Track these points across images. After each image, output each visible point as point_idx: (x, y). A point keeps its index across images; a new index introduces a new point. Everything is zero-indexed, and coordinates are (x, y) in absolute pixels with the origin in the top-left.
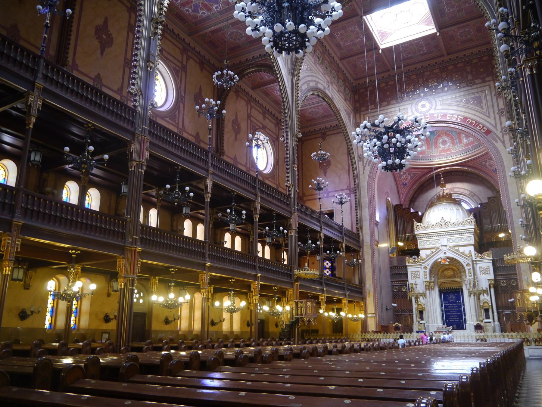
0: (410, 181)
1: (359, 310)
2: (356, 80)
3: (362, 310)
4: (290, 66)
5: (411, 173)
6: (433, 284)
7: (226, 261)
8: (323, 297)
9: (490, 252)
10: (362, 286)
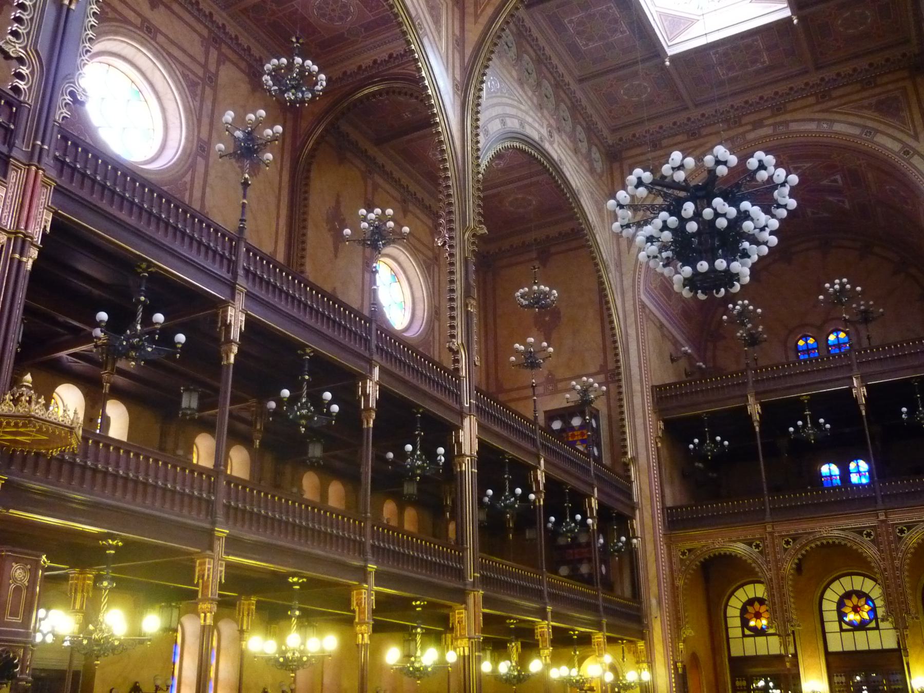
1: (634, 660)
2: (614, 130)
3: (643, 662)
4: (458, 77)
7: (273, 524)
8: (544, 627)
10: (640, 603)
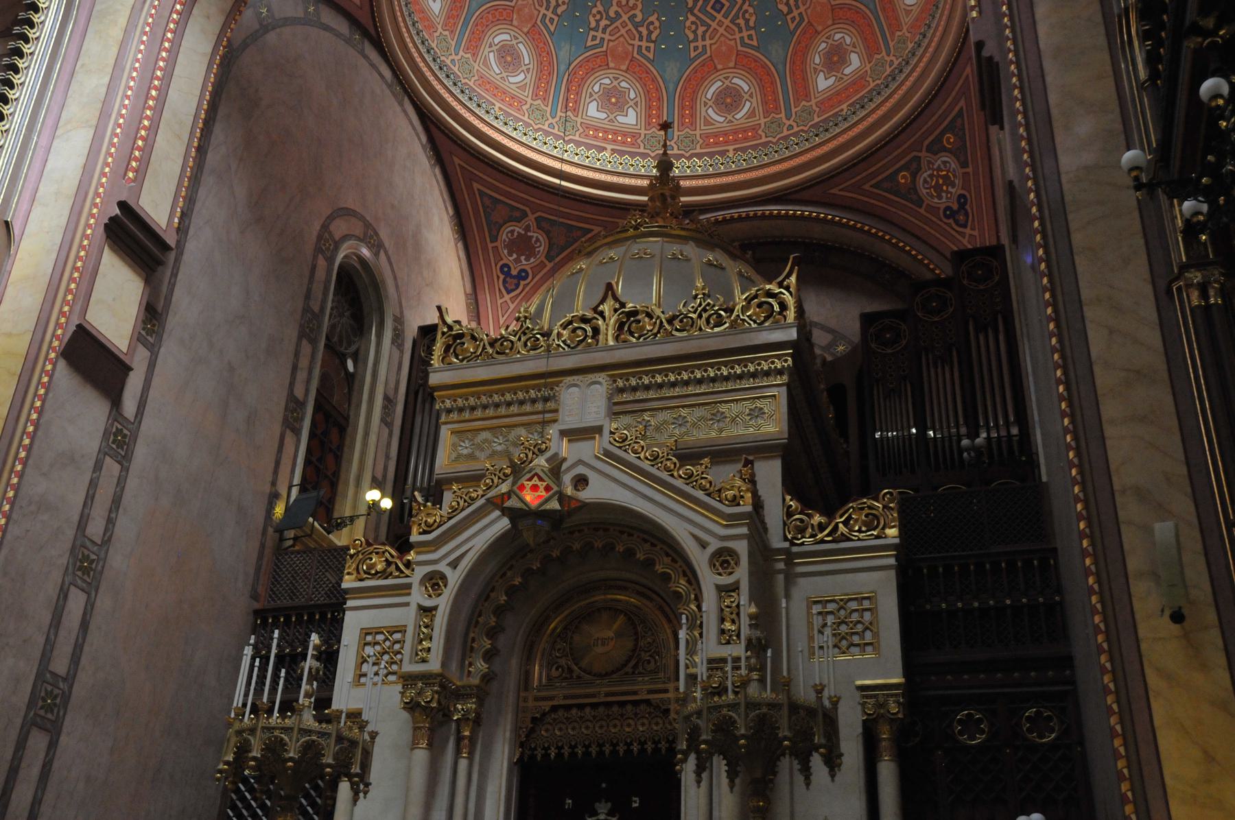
0: (542, 265)
5: (553, 223)
6: (471, 705)
9: (884, 503)
